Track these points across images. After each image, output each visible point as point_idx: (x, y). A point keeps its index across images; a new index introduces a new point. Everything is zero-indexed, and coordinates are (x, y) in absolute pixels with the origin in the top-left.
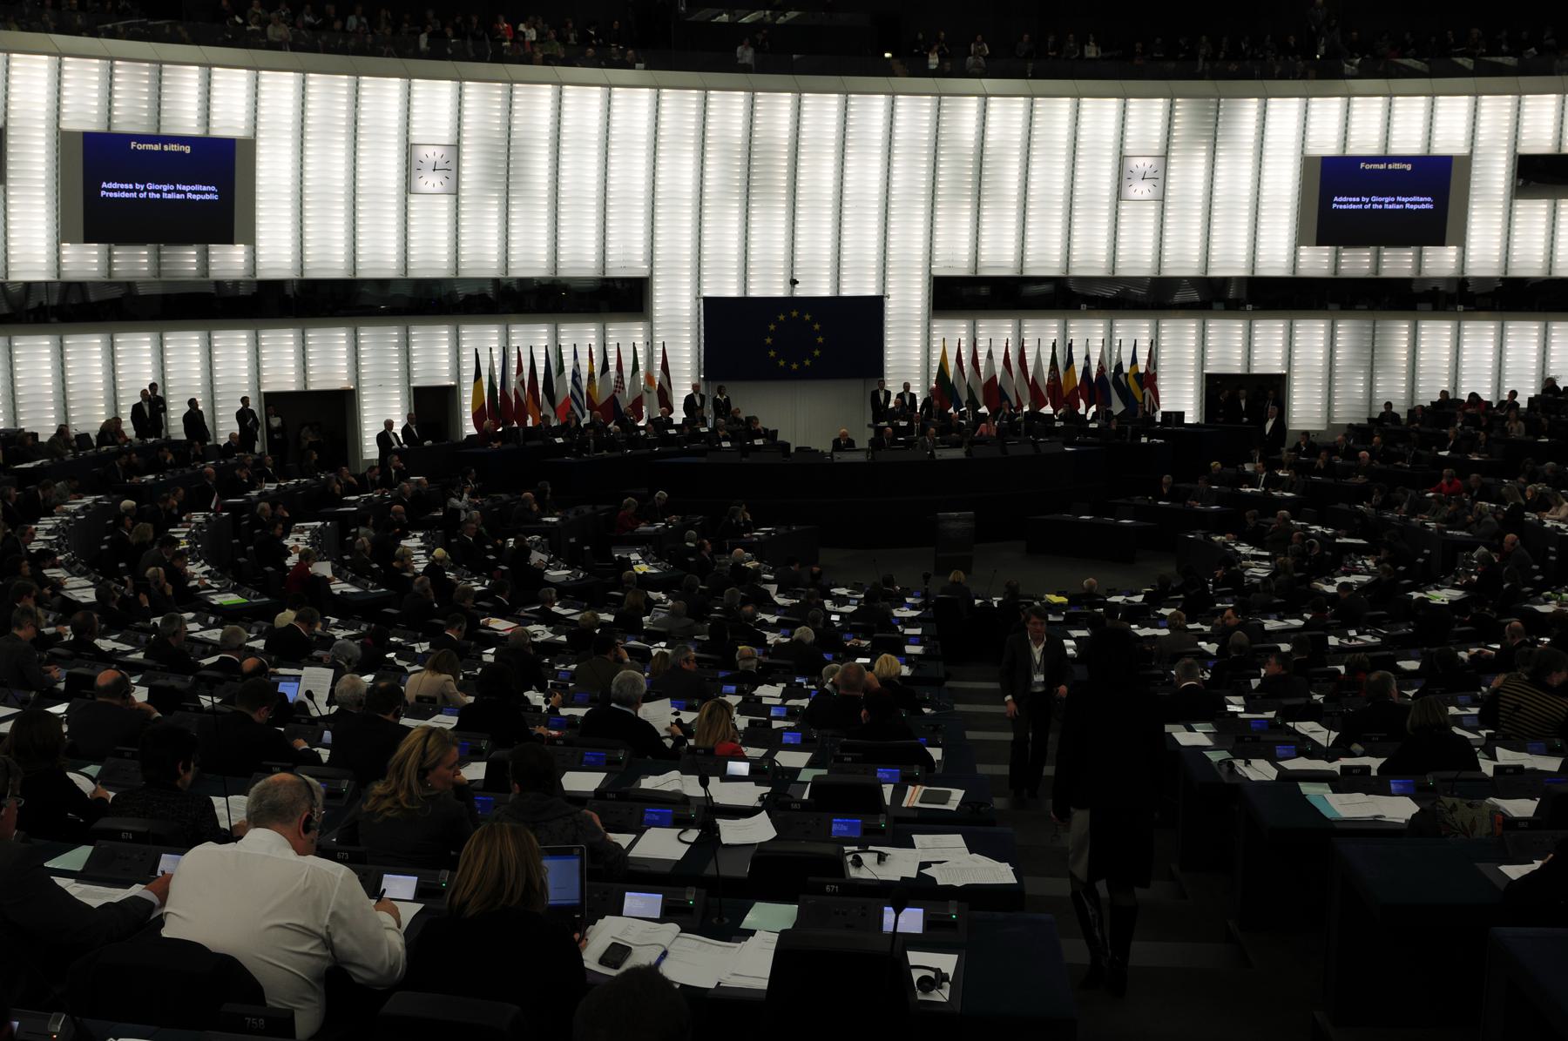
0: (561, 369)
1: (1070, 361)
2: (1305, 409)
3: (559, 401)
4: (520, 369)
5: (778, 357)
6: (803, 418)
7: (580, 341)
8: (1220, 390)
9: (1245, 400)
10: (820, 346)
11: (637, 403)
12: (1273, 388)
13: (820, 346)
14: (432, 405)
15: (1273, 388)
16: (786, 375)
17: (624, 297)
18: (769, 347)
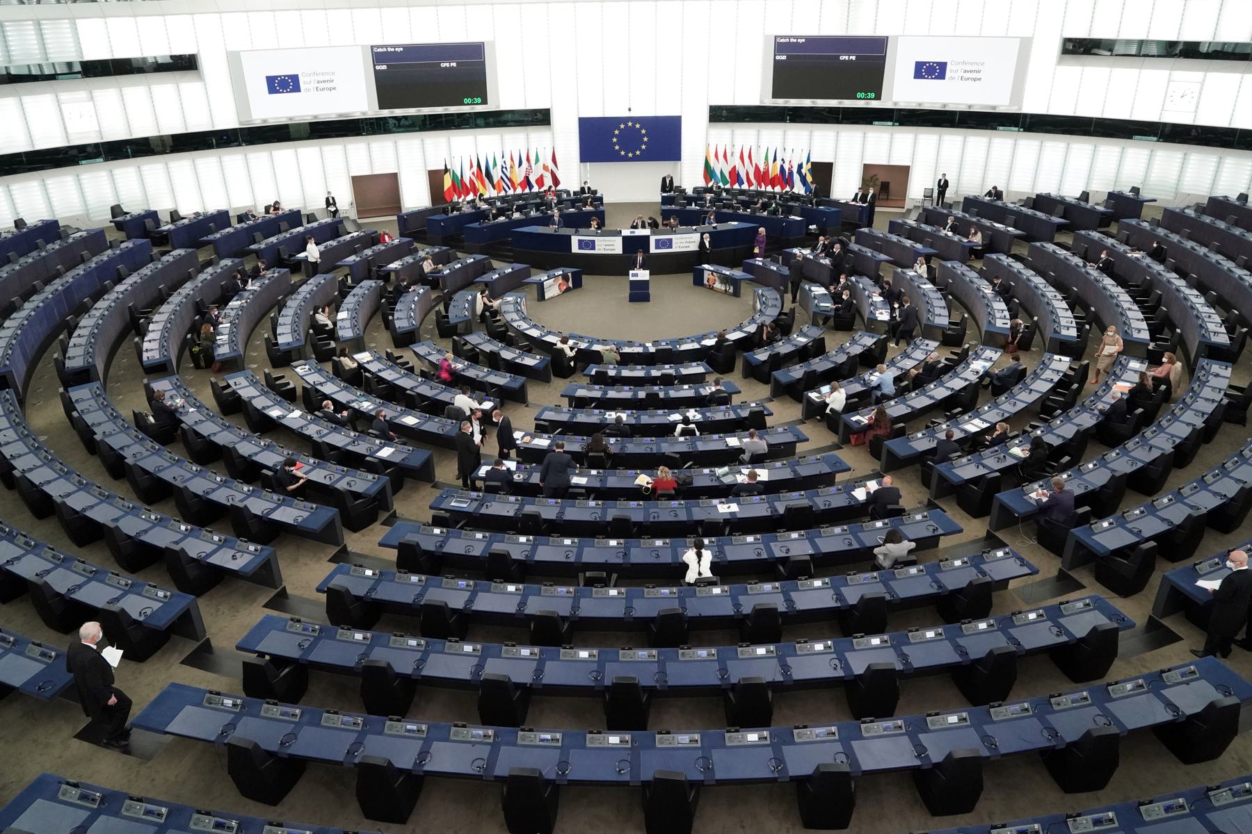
0: (495, 164)
1: (775, 160)
2: (918, 188)
3: (495, 182)
4: (471, 166)
5: (620, 149)
6: (630, 185)
7: (513, 141)
8: (870, 173)
9: (884, 182)
10: (645, 143)
11: (540, 181)
12: (904, 171)
13: (645, 143)
14: (435, 178)
15: (904, 171)
16: (625, 159)
17: (540, 118)
18: (615, 144)
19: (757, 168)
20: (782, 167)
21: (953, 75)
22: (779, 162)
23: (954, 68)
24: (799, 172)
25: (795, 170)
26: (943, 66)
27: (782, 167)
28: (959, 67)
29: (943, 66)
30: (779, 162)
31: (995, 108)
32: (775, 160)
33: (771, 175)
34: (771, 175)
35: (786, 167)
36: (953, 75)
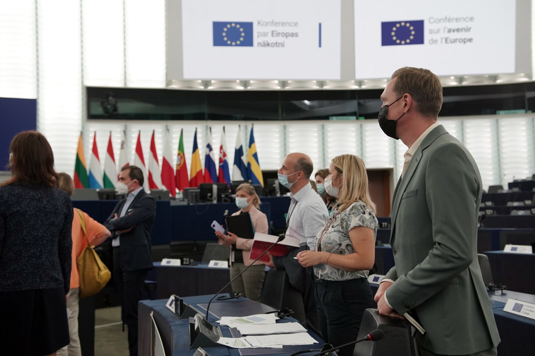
1: (195, 147)
19: (166, 164)
20: (209, 160)
21: (435, 37)
22: (202, 151)
23: (435, 26)
24: (238, 161)
25: (231, 159)
26: (419, 25)
27: (208, 159)
28: (441, 26)
29: (419, 25)
30: (202, 151)
31: (495, 77)
32: (195, 147)
33: (190, 173)
34: (190, 173)
35: (216, 156)
36: (435, 37)
